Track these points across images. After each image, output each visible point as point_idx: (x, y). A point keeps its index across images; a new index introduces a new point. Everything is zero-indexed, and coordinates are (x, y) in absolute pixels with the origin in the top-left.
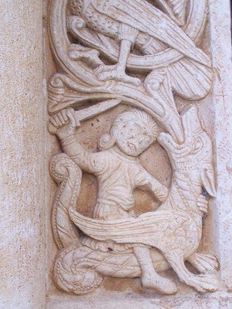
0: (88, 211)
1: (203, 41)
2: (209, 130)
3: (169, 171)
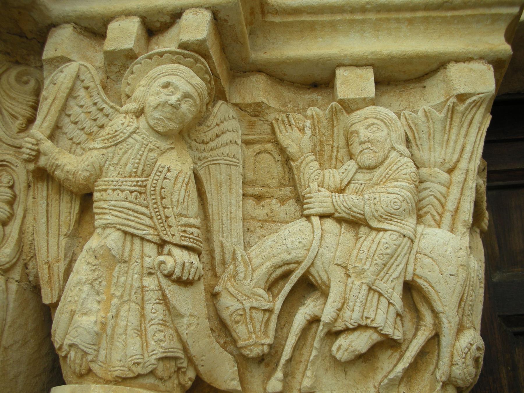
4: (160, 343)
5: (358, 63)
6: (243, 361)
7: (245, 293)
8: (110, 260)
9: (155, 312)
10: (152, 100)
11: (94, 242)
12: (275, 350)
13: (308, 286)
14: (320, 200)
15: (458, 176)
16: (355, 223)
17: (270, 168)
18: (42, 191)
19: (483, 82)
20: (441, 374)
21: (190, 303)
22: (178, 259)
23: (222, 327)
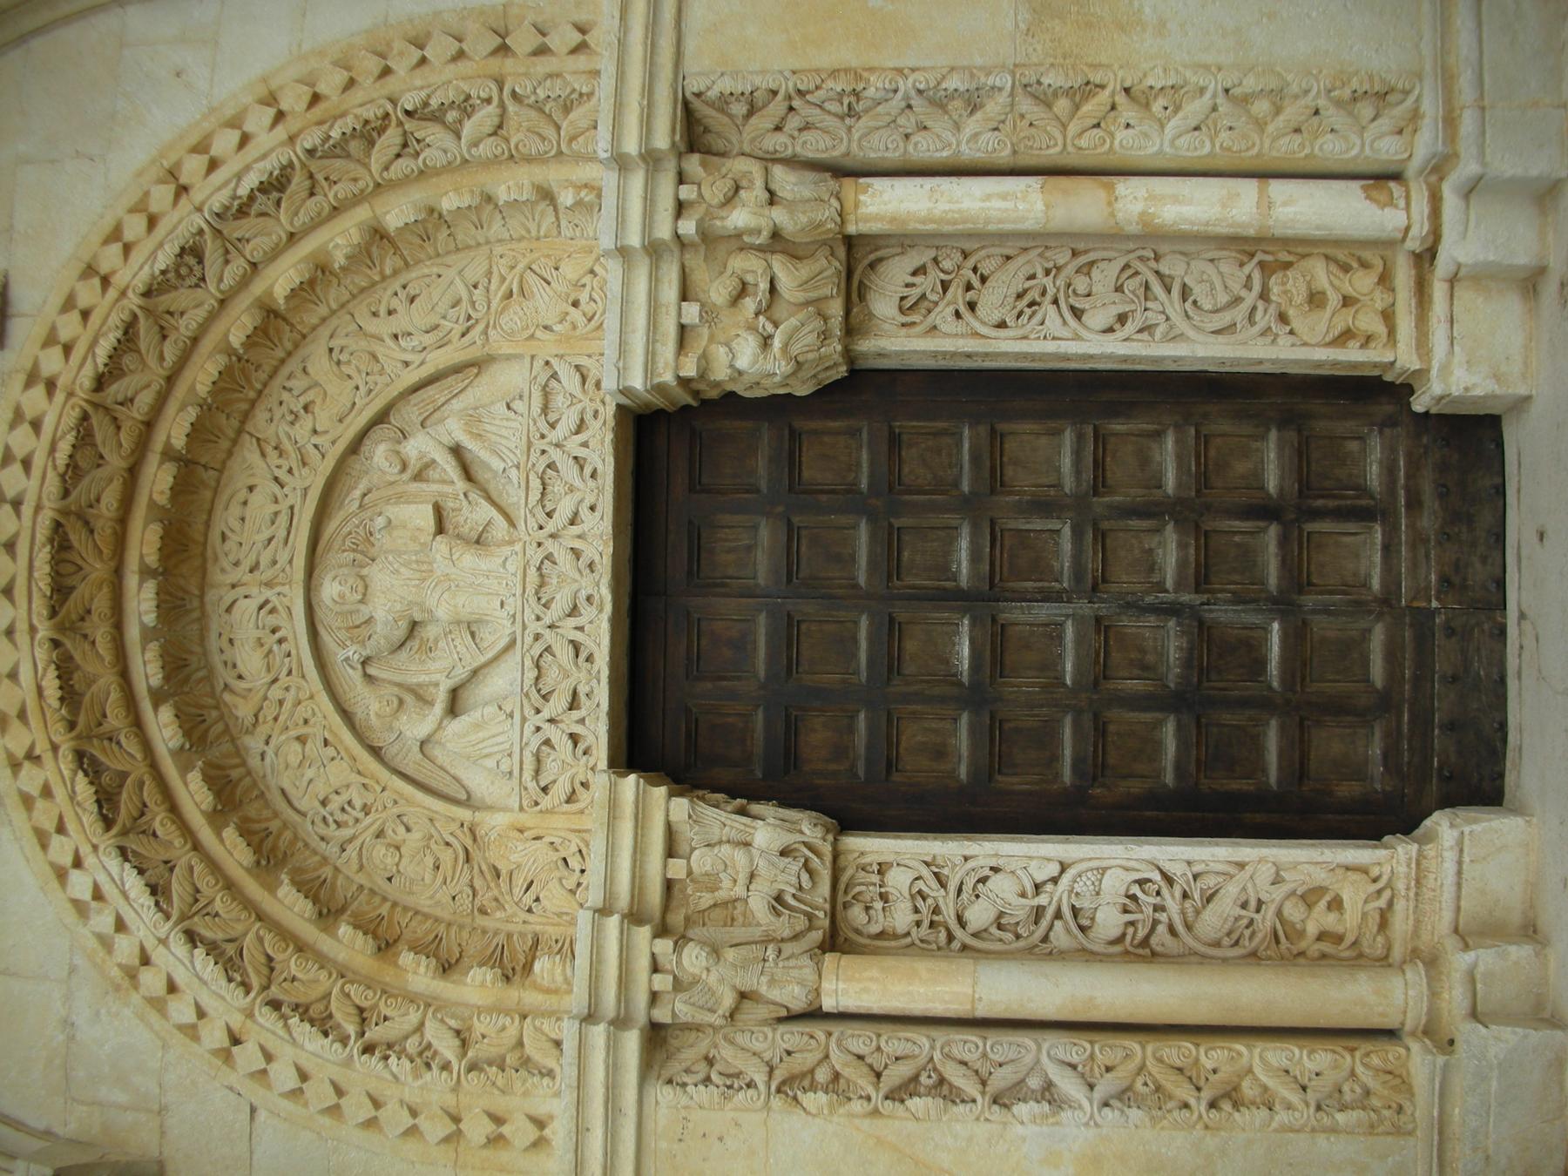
0: (1339, 939)
1: (1241, 866)
2: (1295, 866)
3: (1320, 891)
4: (805, 960)
5: (665, 866)
6: (810, 928)
8: (772, 982)
9: (792, 963)
10: (704, 963)
11: (763, 989)
12: (806, 914)
13: (779, 898)
14: (740, 891)
15: (728, 822)
16: (752, 876)
17: (718, 914)
18: (737, 1016)
19: (680, 806)
20: (821, 842)
21: (788, 948)
22: (771, 954)
23: (796, 937)
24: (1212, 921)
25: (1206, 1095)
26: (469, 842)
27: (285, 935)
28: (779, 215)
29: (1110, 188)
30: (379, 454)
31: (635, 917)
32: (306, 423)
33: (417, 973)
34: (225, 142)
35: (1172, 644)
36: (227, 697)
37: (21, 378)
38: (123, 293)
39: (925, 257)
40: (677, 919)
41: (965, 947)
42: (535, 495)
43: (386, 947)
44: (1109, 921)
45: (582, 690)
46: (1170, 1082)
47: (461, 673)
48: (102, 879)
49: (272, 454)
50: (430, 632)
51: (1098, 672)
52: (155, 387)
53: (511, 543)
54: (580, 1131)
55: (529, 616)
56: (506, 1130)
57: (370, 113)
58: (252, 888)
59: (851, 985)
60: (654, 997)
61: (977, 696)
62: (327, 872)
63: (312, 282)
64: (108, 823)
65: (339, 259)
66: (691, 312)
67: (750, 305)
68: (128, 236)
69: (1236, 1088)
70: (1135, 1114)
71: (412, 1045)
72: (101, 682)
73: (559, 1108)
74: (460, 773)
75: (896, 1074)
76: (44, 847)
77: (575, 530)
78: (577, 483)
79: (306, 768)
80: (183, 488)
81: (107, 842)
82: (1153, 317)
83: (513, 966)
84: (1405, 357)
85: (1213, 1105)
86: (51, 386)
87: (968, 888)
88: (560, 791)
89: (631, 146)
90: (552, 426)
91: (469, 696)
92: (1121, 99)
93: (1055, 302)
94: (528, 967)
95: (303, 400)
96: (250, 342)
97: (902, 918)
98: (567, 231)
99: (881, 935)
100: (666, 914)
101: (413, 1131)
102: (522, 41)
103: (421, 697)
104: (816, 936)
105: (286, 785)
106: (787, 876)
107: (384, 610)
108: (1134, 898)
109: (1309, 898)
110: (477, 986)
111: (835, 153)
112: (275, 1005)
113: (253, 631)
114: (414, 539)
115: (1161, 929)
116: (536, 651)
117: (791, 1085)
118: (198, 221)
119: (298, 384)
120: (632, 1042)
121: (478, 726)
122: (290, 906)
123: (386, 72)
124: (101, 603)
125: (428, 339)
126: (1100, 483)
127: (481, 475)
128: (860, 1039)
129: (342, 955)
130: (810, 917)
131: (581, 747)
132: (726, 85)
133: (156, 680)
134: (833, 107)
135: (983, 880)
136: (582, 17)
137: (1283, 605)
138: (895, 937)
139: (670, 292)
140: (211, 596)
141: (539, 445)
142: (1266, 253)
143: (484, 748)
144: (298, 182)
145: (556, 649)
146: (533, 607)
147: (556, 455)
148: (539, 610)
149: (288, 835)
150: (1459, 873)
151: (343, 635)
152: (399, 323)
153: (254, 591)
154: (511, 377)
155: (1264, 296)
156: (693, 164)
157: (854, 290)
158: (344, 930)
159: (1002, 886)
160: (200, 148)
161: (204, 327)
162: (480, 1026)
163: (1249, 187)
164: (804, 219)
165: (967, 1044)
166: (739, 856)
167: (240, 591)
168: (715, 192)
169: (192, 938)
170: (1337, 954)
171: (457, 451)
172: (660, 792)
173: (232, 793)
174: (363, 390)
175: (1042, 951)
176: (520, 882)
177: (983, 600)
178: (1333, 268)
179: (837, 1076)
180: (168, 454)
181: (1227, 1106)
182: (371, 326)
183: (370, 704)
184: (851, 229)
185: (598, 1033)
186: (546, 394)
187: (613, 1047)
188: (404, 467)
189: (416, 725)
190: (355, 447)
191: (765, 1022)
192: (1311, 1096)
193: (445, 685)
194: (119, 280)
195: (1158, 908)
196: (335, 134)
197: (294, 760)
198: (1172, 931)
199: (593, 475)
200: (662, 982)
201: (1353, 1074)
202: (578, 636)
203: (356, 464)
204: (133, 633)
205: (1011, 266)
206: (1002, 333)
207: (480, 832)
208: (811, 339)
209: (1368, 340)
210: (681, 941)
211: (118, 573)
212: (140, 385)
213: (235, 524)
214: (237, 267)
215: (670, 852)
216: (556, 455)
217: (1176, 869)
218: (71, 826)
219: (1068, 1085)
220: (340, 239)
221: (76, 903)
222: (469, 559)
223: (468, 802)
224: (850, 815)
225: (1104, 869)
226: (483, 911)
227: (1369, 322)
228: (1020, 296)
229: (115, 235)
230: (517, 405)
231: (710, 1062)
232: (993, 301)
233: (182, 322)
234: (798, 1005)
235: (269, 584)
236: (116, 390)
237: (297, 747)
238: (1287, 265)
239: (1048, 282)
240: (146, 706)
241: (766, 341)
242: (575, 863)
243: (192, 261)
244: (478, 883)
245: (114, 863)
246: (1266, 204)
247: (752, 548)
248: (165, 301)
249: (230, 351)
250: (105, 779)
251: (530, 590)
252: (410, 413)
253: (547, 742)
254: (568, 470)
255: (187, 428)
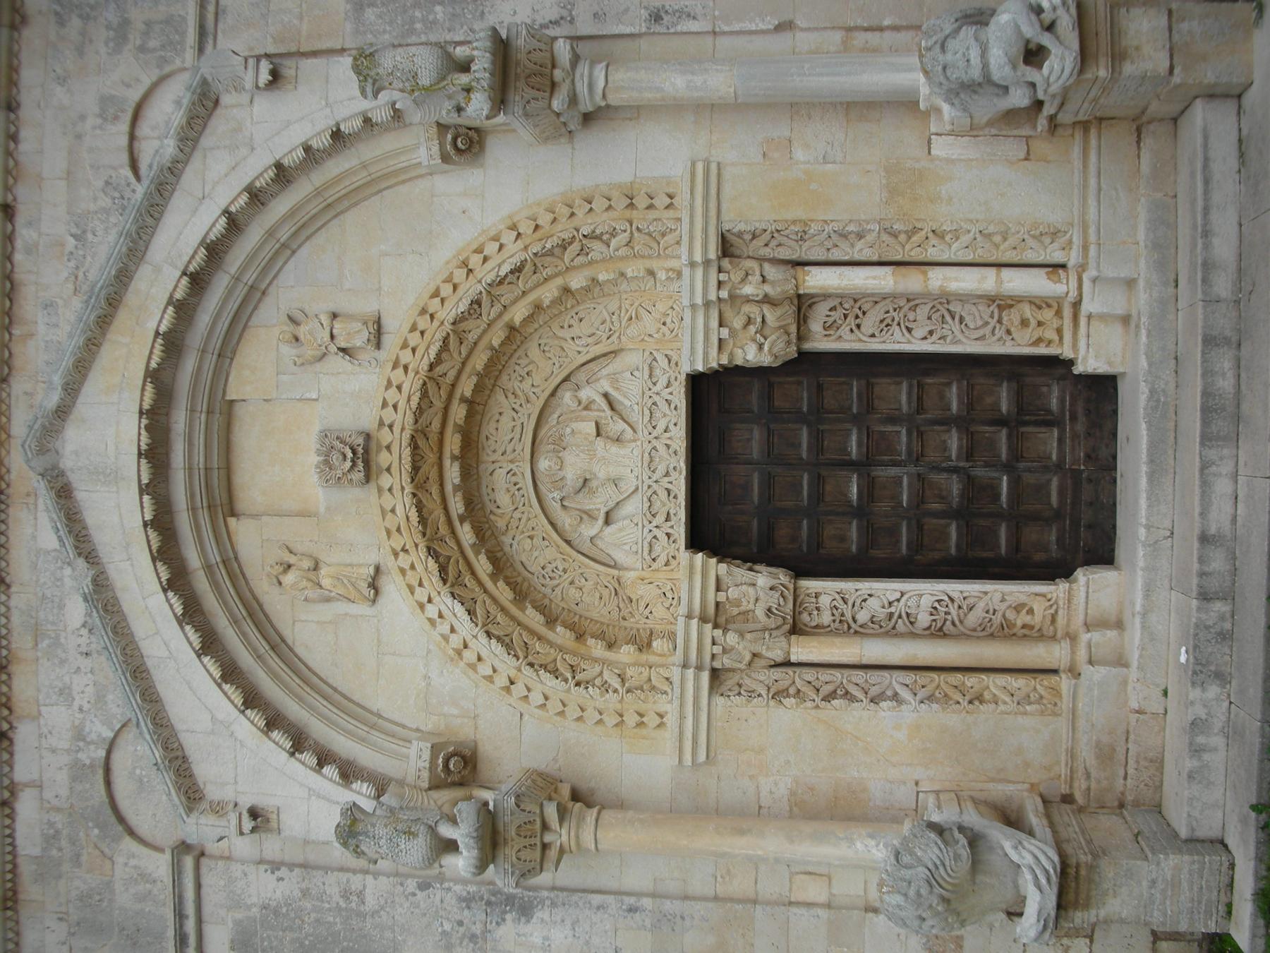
0: (1032, 628)
1: (986, 593)
2: (1011, 593)
3: (1023, 605)
4: (783, 639)
7: (772, 623)
8: (768, 649)
13: (769, 610)
14: (751, 606)
16: (757, 600)
19: (723, 567)
21: (774, 633)
22: (767, 635)
23: (777, 628)
24: (973, 619)
25: (968, 698)
26: (617, 586)
27: (532, 633)
28: (767, 288)
29: (925, 273)
30: (567, 397)
31: (703, 619)
32: (529, 381)
33: (596, 648)
34: (491, 248)
35: (955, 487)
36: (492, 517)
37: (391, 364)
38: (442, 323)
39: (836, 302)
40: (722, 620)
41: (856, 632)
42: (647, 418)
43: (580, 637)
44: (924, 619)
45: (672, 512)
46: (950, 692)
47: (611, 504)
48: (443, 608)
49: (511, 397)
50: (594, 484)
51: (919, 500)
52: (457, 367)
53: (635, 441)
54: (682, 717)
55: (645, 477)
56: (644, 719)
57: (566, 235)
58: (514, 610)
59: (803, 650)
60: (713, 656)
61: (861, 512)
62: (546, 602)
63: (532, 315)
64: (445, 581)
65: (547, 302)
66: (725, 333)
67: (752, 329)
68: (443, 294)
69: (981, 695)
70: (935, 706)
71: (598, 682)
72: (436, 513)
73: (671, 710)
74: (611, 552)
75: (826, 689)
76: (412, 593)
77: (667, 435)
78: (668, 412)
79: (535, 552)
80: (470, 415)
81: (445, 590)
82: (945, 332)
83: (643, 644)
84: (1067, 353)
85: (970, 702)
86: (406, 368)
87: (857, 604)
88: (662, 560)
89: (698, 257)
90: (655, 384)
91: (614, 516)
92: (931, 235)
93: (899, 324)
94: (649, 645)
95: (526, 370)
96: (503, 344)
97: (826, 618)
98: (659, 288)
99: (817, 627)
100: (717, 617)
101: (600, 722)
102: (641, 202)
103: (591, 516)
104: (787, 627)
105: (524, 559)
106: (773, 600)
107: (571, 474)
108: (935, 608)
109: (1018, 608)
110: (626, 653)
111: (794, 257)
112: (531, 665)
113: (504, 484)
114: (586, 439)
115: (948, 623)
116: (649, 494)
117: (779, 695)
118: (480, 288)
119: (523, 362)
120: (705, 676)
121: (620, 530)
122: (532, 617)
123: (573, 214)
124: (433, 474)
125: (590, 340)
126: (920, 409)
127: (618, 407)
128: (809, 674)
129: (559, 642)
130: (784, 619)
131: (672, 539)
132: (742, 227)
133: (461, 510)
134: (794, 237)
135: (865, 600)
136: (671, 190)
137: (1009, 468)
138: (824, 627)
139: (714, 323)
140: (482, 467)
141: (648, 393)
142: (1002, 303)
143: (624, 541)
144: (528, 268)
145: (659, 492)
146: (647, 473)
147: (656, 398)
148: (650, 473)
149: (526, 584)
150: (1087, 597)
151: (549, 485)
152: (576, 331)
153: (504, 465)
154: (632, 359)
155: (1000, 321)
156: (726, 263)
157: (802, 319)
158: (559, 629)
159: (872, 602)
160: (479, 251)
161: (480, 338)
162: (629, 672)
163: (992, 272)
164: (779, 290)
165: (859, 676)
166: (751, 590)
167: (497, 465)
168: (736, 277)
169: (489, 634)
170: (1031, 634)
171: (606, 396)
172: (714, 560)
173: (500, 565)
174: (557, 365)
175: (892, 634)
176: (642, 605)
177: (863, 465)
178: (1033, 307)
179: (799, 691)
180: (463, 400)
181: (977, 703)
182: (560, 333)
183: (566, 520)
184: (801, 292)
185: (690, 673)
186: (651, 368)
187: (697, 679)
188: (580, 403)
189: (589, 530)
190: (553, 394)
191: (764, 667)
192: (1015, 699)
193: (606, 509)
194: (441, 315)
195: (946, 613)
196: (548, 246)
197: (527, 547)
198: (953, 624)
199: (676, 408)
200: (717, 649)
201: (1035, 689)
202: (670, 486)
203: (554, 401)
204: (449, 488)
205: (878, 307)
206: (873, 339)
207: (622, 581)
208: (782, 345)
209: (1050, 342)
210: (725, 630)
211: (440, 458)
212: (449, 368)
213: (494, 432)
214: (497, 308)
215: (718, 589)
216: (656, 398)
217: (955, 595)
218: (425, 584)
219: (905, 694)
220: (548, 293)
221: (429, 619)
222: (614, 449)
223: (615, 567)
224: (801, 570)
225: (922, 595)
226: (624, 619)
227: (1050, 334)
228: (882, 321)
229: (436, 294)
230: (636, 373)
231: (740, 686)
232: (869, 324)
233: (470, 336)
234: (779, 659)
235: (512, 461)
236: (439, 370)
237: (529, 541)
238: (1011, 306)
239: (895, 314)
240: (457, 523)
241: (761, 347)
242: (669, 595)
243: (476, 306)
244: (621, 605)
245: (449, 600)
246: (999, 281)
247: (751, 440)
248: (463, 326)
249: (492, 348)
250: (441, 559)
251: (646, 464)
252: (581, 377)
253: (655, 537)
254: (663, 406)
255: (472, 387)
